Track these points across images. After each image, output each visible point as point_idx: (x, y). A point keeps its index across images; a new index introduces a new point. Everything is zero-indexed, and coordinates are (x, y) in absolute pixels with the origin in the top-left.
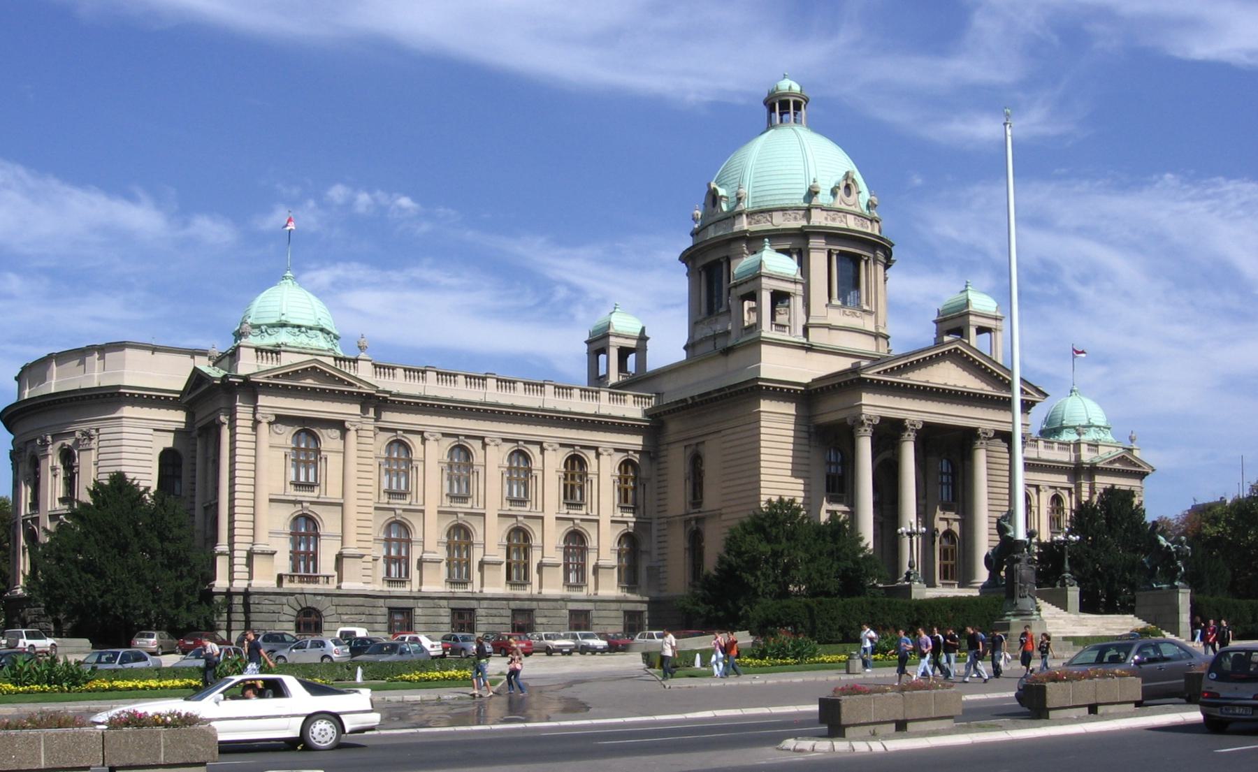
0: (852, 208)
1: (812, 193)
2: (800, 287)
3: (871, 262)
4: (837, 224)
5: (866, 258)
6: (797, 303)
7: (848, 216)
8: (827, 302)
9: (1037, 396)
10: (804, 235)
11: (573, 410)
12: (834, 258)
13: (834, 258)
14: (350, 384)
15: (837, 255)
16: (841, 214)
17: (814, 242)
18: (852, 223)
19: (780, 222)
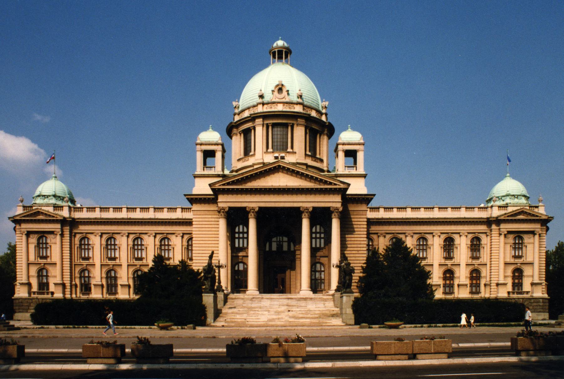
0: (284, 100)
1: (261, 96)
2: (220, 147)
3: (295, 126)
4: (273, 110)
5: (291, 124)
6: (219, 155)
7: (279, 105)
8: (265, 150)
9: (342, 185)
10: (253, 118)
11: (172, 218)
12: (270, 128)
13: (270, 128)
14: (53, 217)
15: (271, 125)
16: (275, 104)
17: (259, 121)
18: (280, 108)
19: (246, 114)
